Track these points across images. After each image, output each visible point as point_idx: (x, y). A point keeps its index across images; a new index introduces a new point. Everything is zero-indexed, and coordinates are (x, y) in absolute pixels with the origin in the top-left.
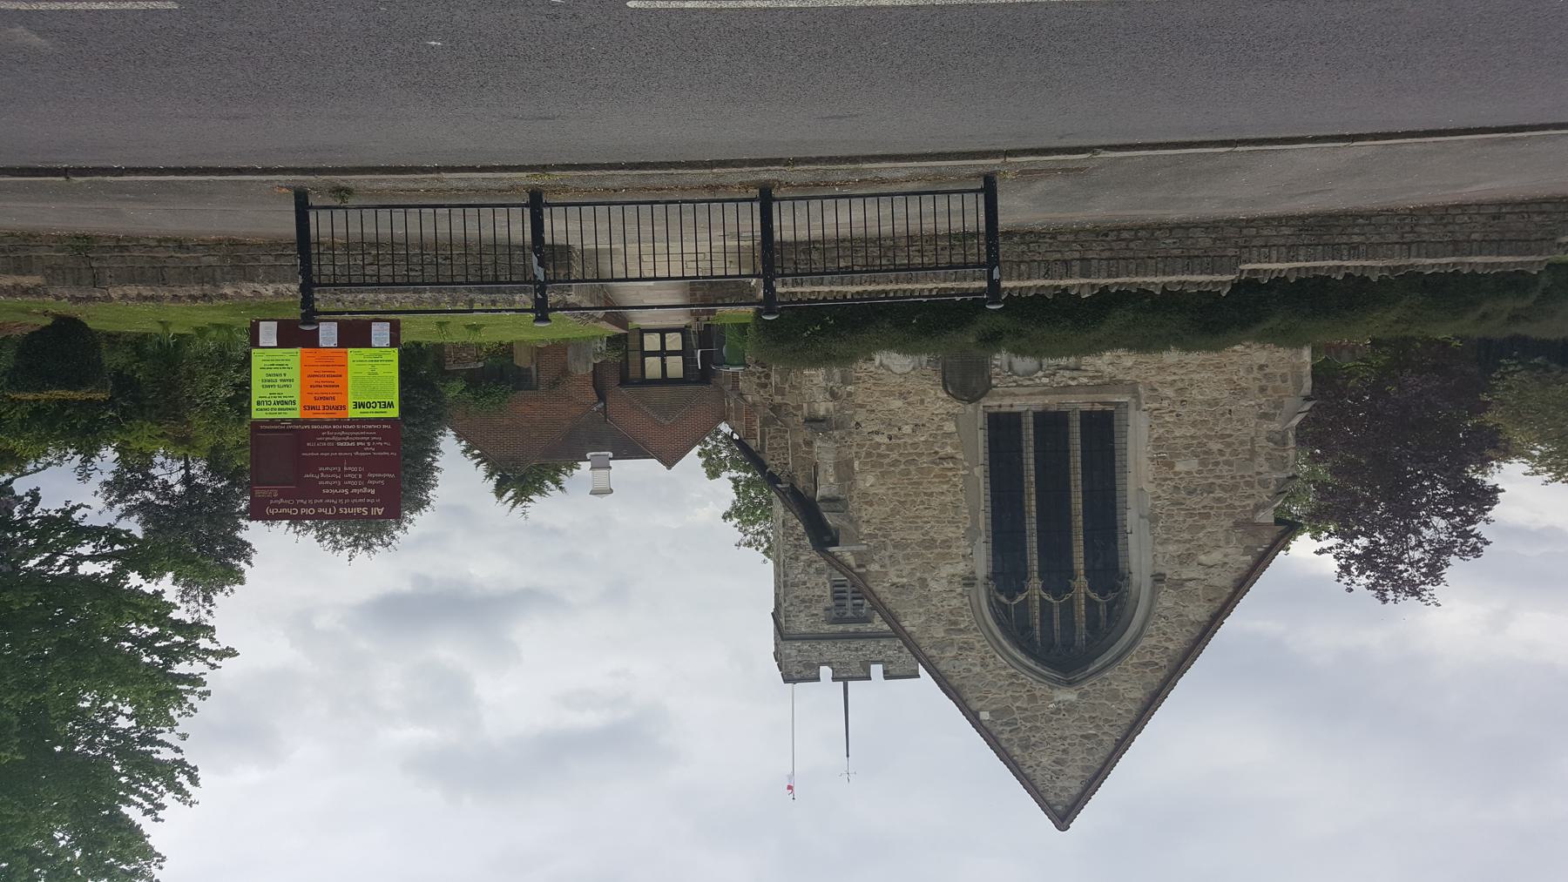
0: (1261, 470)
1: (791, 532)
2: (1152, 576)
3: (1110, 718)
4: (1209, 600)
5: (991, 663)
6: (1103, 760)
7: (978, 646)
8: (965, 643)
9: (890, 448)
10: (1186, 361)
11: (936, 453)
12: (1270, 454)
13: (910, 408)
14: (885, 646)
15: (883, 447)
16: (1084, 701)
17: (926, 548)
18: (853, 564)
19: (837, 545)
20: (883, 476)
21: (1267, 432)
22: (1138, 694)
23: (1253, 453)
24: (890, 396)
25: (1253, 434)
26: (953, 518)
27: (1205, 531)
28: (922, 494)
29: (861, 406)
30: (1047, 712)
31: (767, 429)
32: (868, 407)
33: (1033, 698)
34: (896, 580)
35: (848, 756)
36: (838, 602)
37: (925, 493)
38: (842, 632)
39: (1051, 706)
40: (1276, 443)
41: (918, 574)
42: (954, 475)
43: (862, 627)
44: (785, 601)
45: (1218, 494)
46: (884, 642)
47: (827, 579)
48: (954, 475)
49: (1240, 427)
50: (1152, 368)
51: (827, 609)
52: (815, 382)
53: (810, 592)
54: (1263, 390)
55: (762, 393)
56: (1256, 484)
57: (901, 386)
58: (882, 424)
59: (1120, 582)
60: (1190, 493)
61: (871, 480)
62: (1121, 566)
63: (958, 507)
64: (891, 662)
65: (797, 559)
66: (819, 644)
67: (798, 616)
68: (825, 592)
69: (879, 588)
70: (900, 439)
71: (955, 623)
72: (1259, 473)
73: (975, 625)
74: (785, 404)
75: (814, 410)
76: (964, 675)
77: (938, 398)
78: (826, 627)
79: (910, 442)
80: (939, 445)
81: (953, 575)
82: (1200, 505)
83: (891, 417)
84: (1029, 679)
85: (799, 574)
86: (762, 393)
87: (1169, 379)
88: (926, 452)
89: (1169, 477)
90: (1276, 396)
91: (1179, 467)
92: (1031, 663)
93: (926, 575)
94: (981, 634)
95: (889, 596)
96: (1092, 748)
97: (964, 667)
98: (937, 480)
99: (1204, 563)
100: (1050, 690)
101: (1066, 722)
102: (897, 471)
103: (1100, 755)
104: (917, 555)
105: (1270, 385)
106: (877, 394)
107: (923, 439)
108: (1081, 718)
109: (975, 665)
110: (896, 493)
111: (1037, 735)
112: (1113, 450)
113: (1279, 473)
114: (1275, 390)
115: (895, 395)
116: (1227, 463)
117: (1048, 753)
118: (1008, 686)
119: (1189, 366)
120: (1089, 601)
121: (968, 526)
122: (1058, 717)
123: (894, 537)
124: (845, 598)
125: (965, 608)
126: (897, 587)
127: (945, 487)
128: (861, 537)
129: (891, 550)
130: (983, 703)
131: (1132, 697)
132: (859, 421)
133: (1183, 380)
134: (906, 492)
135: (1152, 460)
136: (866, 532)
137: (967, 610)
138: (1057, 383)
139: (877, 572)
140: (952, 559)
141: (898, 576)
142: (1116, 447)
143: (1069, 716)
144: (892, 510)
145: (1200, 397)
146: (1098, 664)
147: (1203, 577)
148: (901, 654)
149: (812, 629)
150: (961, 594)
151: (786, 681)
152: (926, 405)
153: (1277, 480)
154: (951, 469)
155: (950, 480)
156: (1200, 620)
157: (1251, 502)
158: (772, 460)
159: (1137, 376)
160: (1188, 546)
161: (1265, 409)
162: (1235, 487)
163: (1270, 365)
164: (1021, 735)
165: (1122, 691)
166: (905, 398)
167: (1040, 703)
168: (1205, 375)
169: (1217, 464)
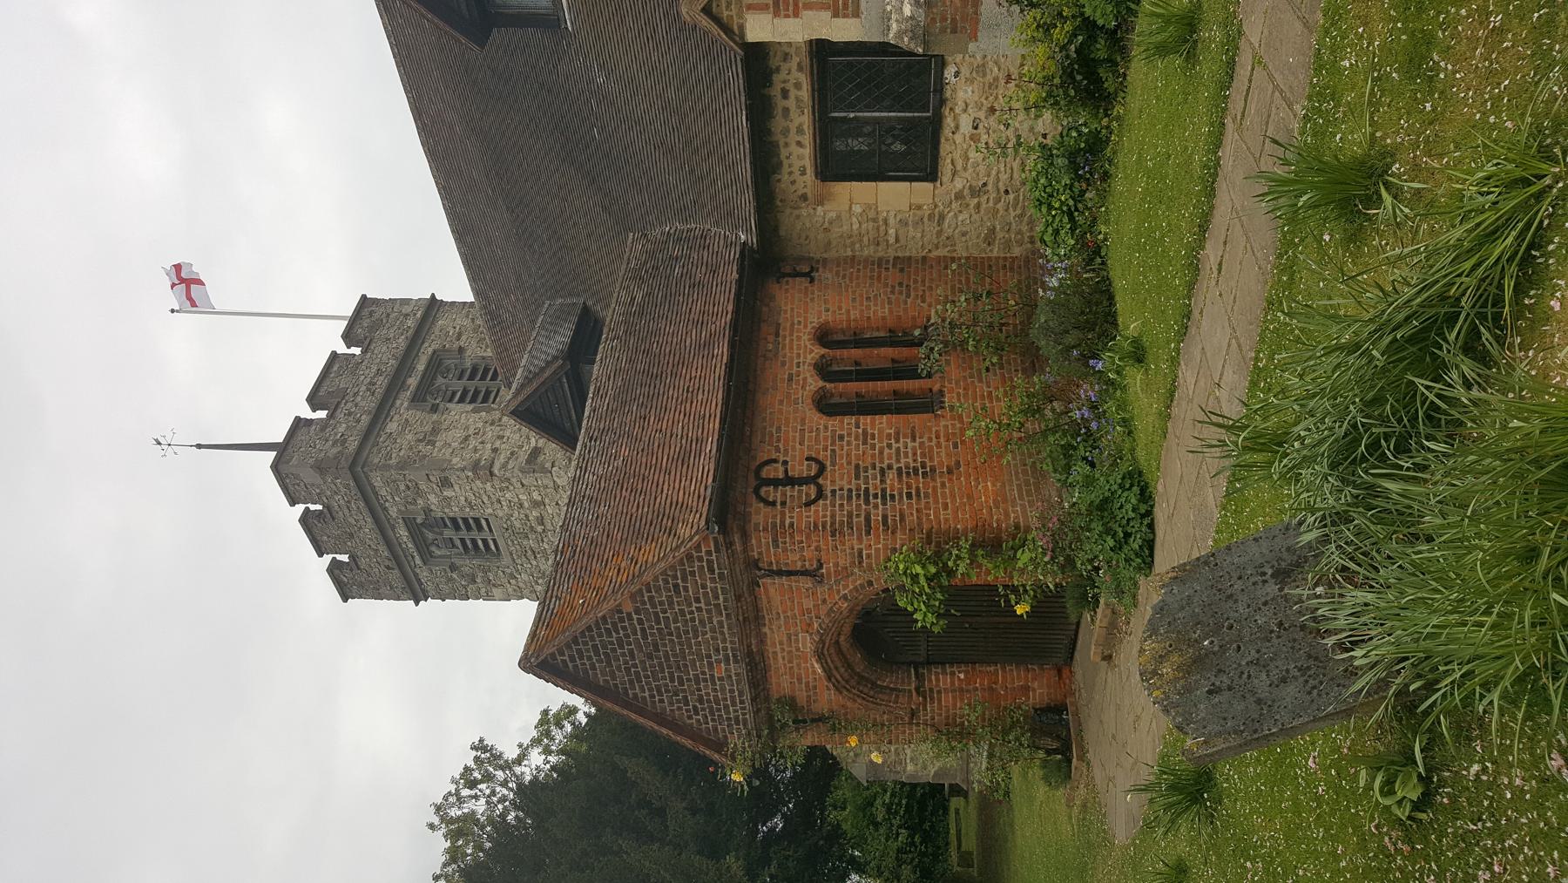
14: (358, 421)
35: (199, 446)
46: (365, 419)
51: (461, 350)
67: (467, 317)
78: (430, 350)
149: (437, 333)
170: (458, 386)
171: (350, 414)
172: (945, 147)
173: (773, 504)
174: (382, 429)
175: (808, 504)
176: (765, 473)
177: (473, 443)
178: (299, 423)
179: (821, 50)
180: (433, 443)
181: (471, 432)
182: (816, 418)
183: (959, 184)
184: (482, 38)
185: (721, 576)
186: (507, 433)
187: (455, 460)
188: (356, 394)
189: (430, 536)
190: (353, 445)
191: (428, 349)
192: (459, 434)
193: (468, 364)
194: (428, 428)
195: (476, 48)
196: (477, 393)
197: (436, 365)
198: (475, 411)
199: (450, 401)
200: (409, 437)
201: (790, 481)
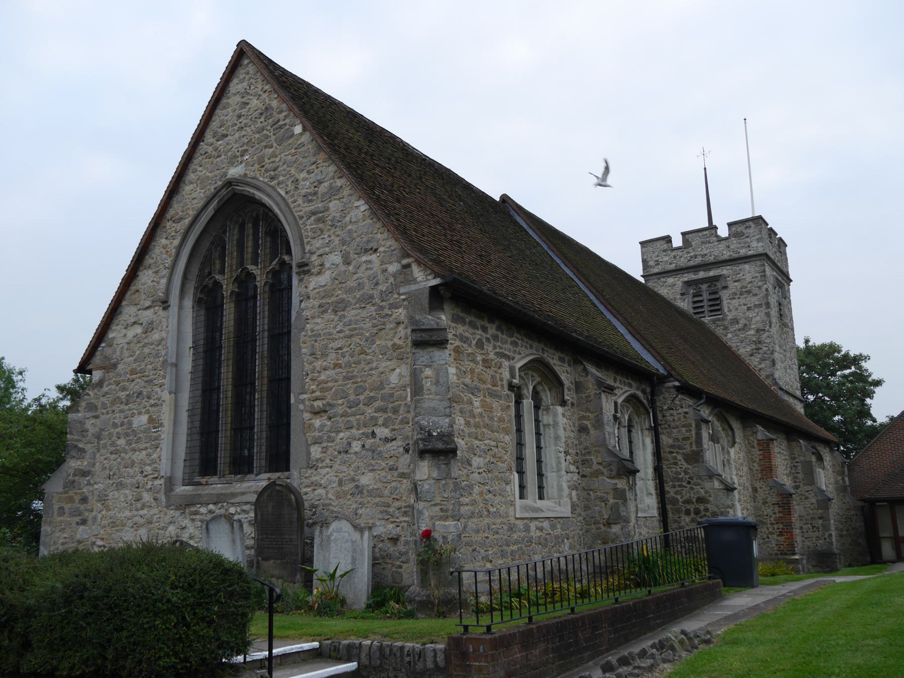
0: (93, 421)
1: (765, 355)
2: (169, 306)
3: (207, 160)
4: (138, 291)
5: (290, 185)
6: (213, 119)
7: (300, 201)
8: (311, 201)
9: (374, 421)
10: (133, 529)
11: (330, 418)
12: (84, 436)
13: (352, 473)
14: (671, 264)
15: (380, 422)
16: (224, 170)
17: (343, 300)
18: (415, 269)
19: (431, 287)
20: (382, 383)
21: (83, 458)
22: (187, 189)
23: (98, 437)
24: (373, 489)
25: (98, 456)
26: (316, 341)
27: (134, 357)
28: (343, 365)
29: (403, 475)
30: (251, 151)
31: (694, 448)
32: (396, 474)
33: (261, 161)
34: (373, 257)
35: (705, 169)
36: (717, 296)
37: (340, 367)
39: (247, 157)
40: (76, 446)
41: (351, 268)
42: (313, 392)
43: (691, 276)
44: (767, 290)
45: (123, 395)
46: (672, 267)
47: (727, 315)
48: (313, 392)
49: (106, 461)
50: (156, 522)
51: (725, 287)
52: (437, 508)
53: (742, 301)
54: (84, 500)
55: (702, 491)
56: (99, 406)
57: (360, 504)
58: (381, 451)
59: (202, 296)
60: (140, 393)
61: (394, 378)
62: (203, 312)
63: (312, 354)
64: (664, 251)
65: (758, 331)
66: (730, 256)
68: (728, 303)
69: (389, 243)
70: (363, 434)
71: (319, 220)
72: (96, 417)
73: (301, 222)
74: (612, 478)
75: (439, 468)
76: (314, 167)
77: (325, 488)
79: (354, 431)
80: (326, 429)
81: (319, 273)
82: (135, 382)
83: (373, 462)
84: (263, 179)
85: (755, 317)
86: (702, 491)
87: (145, 512)
88: (338, 418)
89: (153, 408)
90: (71, 493)
91: (144, 418)
92: (259, 195)
93: (343, 268)
94: (296, 214)
95: (379, 236)
96: (221, 127)
97: (314, 174)
98: (330, 384)
99: (139, 326)
100: (247, 172)
101: (237, 145)
102: (367, 392)
103: (214, 124)
104: (350, 290)
105: (77, 505)
106: (386, 492)
107: (341, 435)
108: (226, 153)
109: (305, 179)
110: (369, 363)
111: (259, 124)
112: (202, 434)
113: (76, 418)
114: (71, 500)
115: (368, 491)
116: (115, 425)
117: (251, 110)
118: (278, 167)
119: (131, 524)
120: (222, 272)
121: (303, 333)
122: (243, 148)
123: (373, 308)
124: (710, 300)
125: (309, 239)
126: (371, 249)
127: (323, 377)
128: (405, 303)
129: (376, 293)
130: (299, 142)
131: (191, 185)
132: (406, 456)
133: (136, 510)
134: (358, 366)
135: (161, 425)
136: (400, 310)
137: (307, 237)
138: (223, 506)
139: (390, 263)
140: (318, 293)
141: (370, 262)
142: (197, 437)
143: (235, 152)
144: (373, 342)
145: (127, 492)
146: (210, 211)
147: (141, 311)
148: (657, 259)
149: (738, 269)
150: (312, 253)
151: (760, 217)
152: (337, 479)
153: (78, 411)
154: (316, 399)
155: (318, 385)
156: (145, 271)
157: (105, 389)
158: (686, 413)
159: (166, 514)
160: (146, 341)
161: (84, 481)
162: (113, 403)
163: (74, 525)
164: (271, 121)
165: (198, 188)
166: (357, 487)
167: (255, 158)
168: (121, 515)
169: (122, 424)
170: (705, 296)
188: (688, 253)
190: (656, 270)
191: (725, 271)
200: (666, 291)
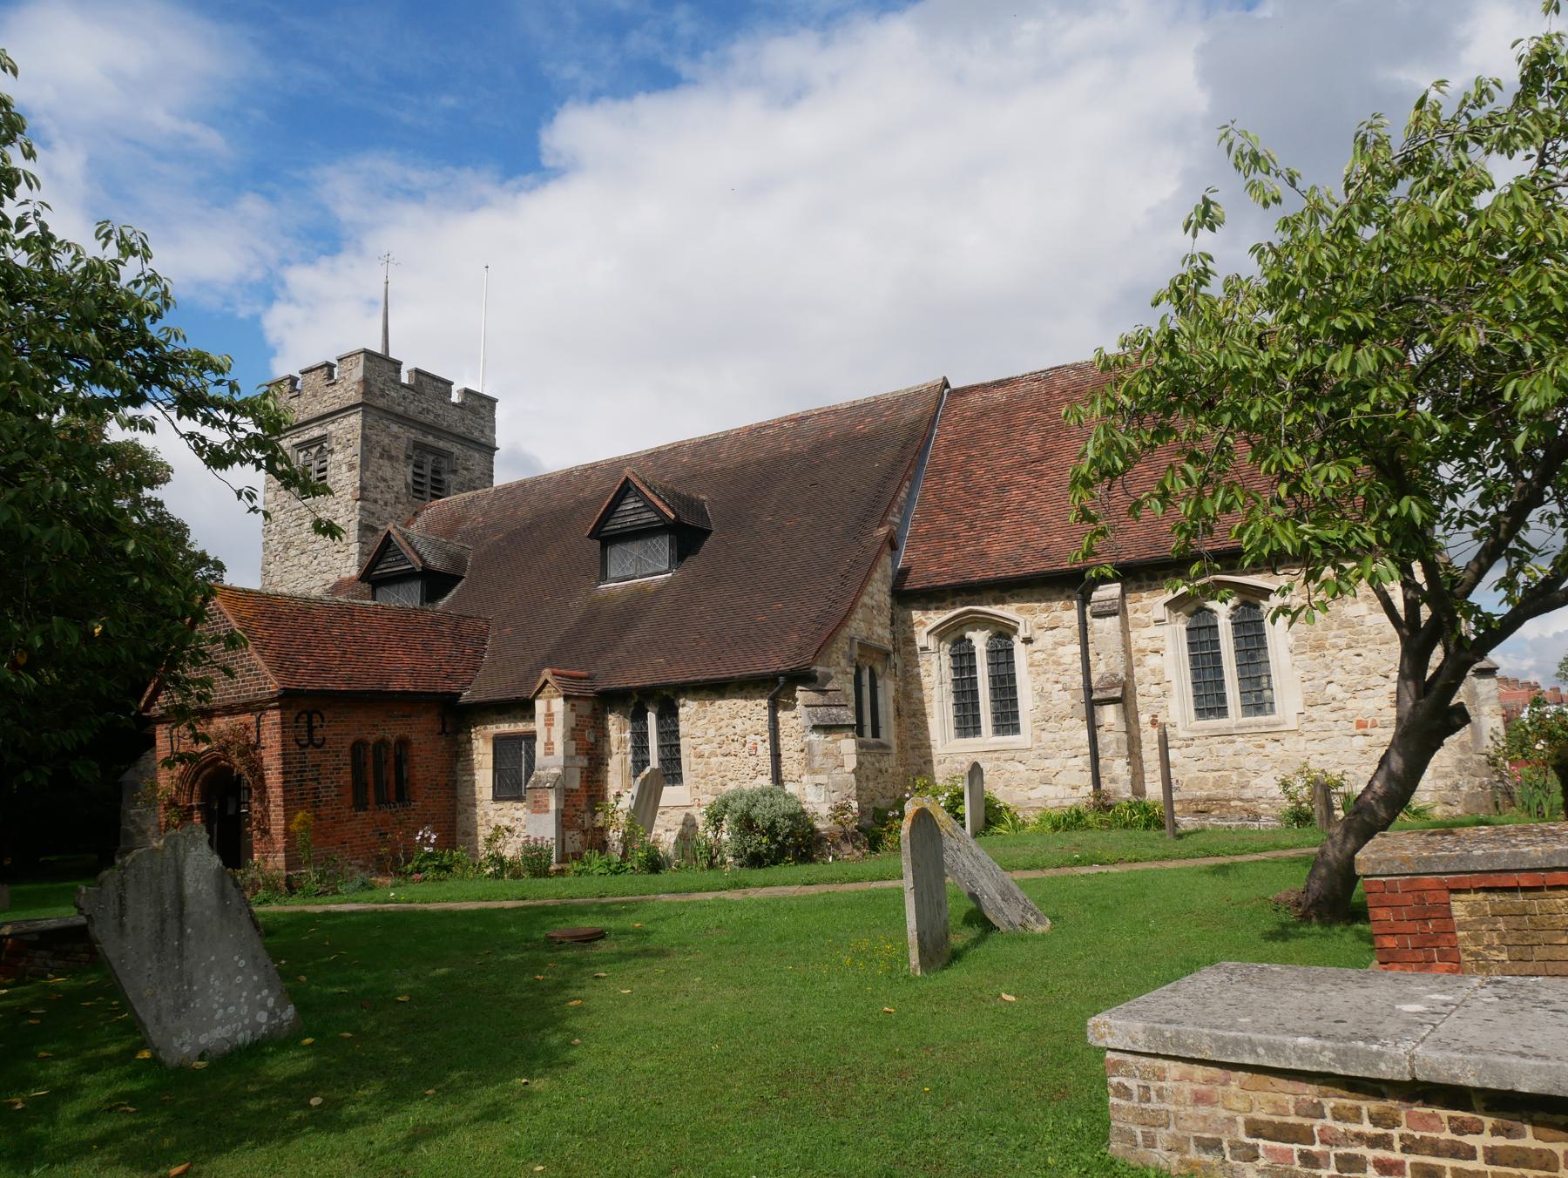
14: (399, 405)
38: (440, 438)
51: (455, 472)
78: (454, 450)
170: (427, 470)
171: (404, 398)
172: (508, 804)
173: (297, 721)
174: (393, 421)
175: (297, 741)
176: (316, 718)
177: (382, 485)
178: (397, 365)
179: (531, 737)
180: (382, 456)
181: (391, 483)
182: (350, 741)
183: (491, 813)
184: (593, 535)
185: (256, 695)
186: (389, 509)
187: (368, 474)
188: (419, 401)
189: (314, 451)
190: (381, 403)
191: (456, 449)
192: (388, 472)
193: (445, 476)
194: (393, 453)
195: (587, 534)
196: (421, 484)
197: (440, 454)
198: (407, 485)
199: (415, 466)
200: (387, 441)
201: (311, 729)
